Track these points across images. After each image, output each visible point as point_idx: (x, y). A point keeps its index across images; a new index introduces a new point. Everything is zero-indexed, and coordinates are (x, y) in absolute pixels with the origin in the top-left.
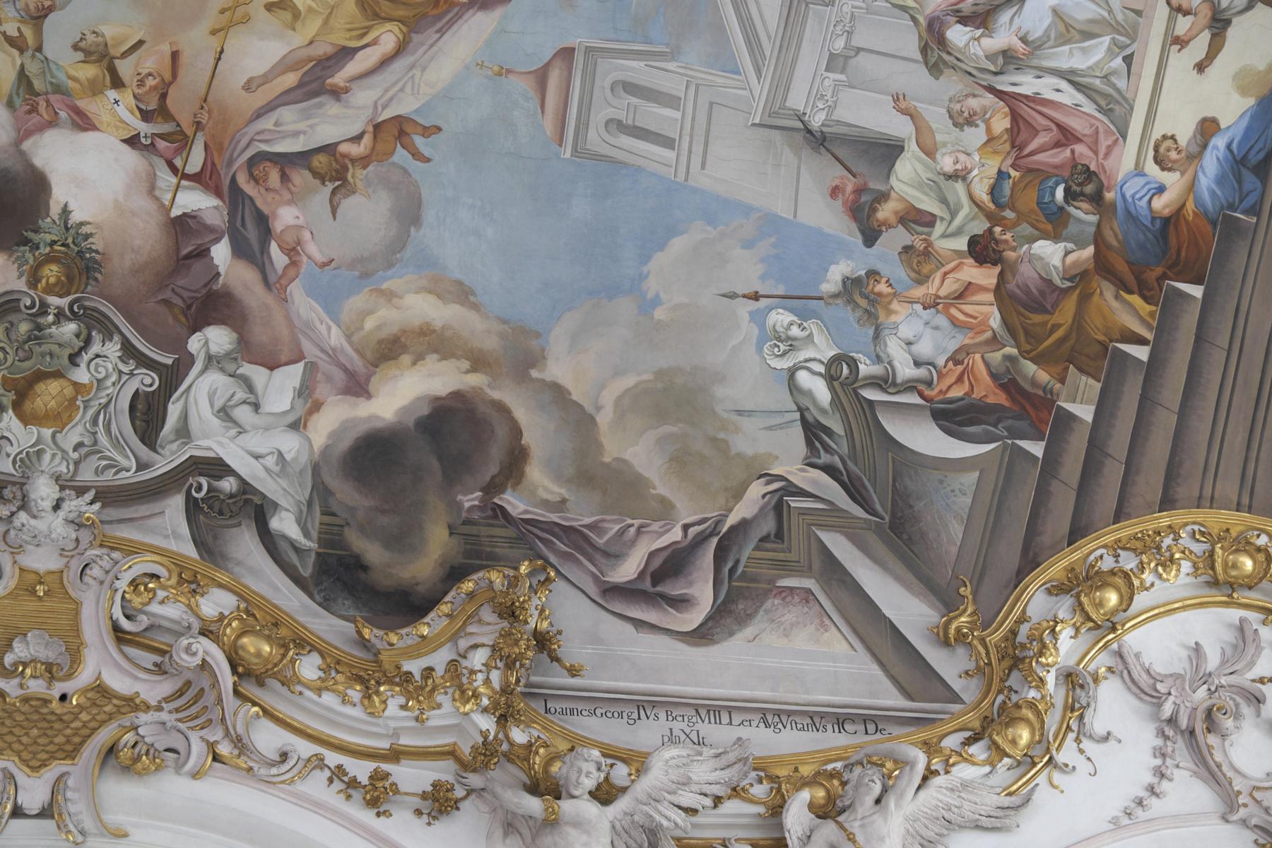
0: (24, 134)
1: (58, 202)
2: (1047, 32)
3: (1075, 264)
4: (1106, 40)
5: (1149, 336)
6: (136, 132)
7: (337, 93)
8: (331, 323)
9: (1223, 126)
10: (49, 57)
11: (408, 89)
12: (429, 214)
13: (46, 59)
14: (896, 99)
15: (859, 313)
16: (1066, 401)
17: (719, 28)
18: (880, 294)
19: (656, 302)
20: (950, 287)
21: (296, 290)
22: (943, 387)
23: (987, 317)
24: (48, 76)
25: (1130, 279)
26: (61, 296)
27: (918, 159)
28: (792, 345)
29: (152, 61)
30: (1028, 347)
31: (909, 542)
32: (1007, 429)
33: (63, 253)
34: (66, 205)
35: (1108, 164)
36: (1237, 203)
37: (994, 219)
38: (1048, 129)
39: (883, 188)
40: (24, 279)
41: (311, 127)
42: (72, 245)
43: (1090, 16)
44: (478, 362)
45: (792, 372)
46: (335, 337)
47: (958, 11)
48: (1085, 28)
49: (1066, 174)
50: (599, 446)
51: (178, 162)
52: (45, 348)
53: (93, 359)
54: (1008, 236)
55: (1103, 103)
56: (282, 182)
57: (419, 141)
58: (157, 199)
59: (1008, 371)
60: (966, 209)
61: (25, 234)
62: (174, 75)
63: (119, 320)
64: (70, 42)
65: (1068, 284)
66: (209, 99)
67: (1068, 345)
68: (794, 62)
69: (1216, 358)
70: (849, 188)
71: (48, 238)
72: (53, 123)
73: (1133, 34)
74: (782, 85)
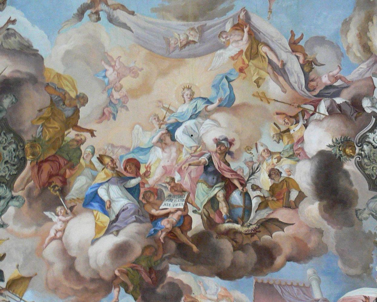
0: (306, 157)
1: (327, 148)
6: (303, 125)
7: (284, 64)
8: (359, 67)
10: (282, 150)
11: (280, 42)
12: (321, 34)
13: (283, 151)
21: (349, 78)
24: (288, 150)
26: (356, 149)
29: (280, 121)
33: (342, 147)
34: (327, 146)
40: (351, 159)
41: (296, 72)
42: (340, 145)
46: (364, 66)
51: (311, 113)
52: (372, 155)
53: (375, 141)
56: (314, 81)
57: (296, 38)
58: (323, 119)
61: (337, 158)
62: (284, 114)
63: (362, 132)
64: (277, 144)
66: (290, 103)
71: (338, 151)
72: (302, 149)
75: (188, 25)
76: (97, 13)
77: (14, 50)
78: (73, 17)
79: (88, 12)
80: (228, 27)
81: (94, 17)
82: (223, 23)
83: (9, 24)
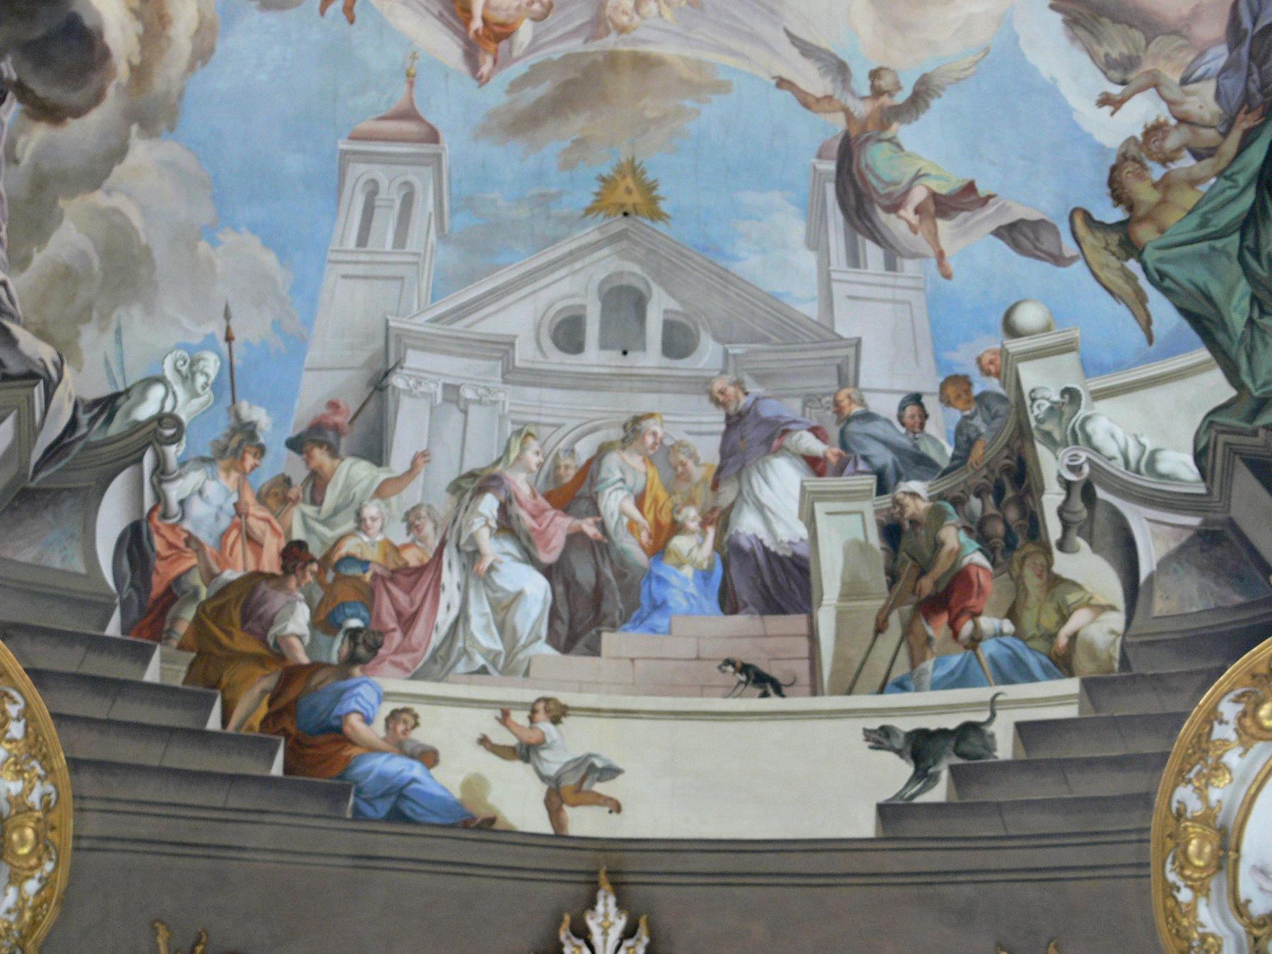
2: (503, 590)
3: (290, 647)
4: (498, 646)
5: (231, 728)
9: (433, 771)
14: (425, 454)
15: (223, 440)
16: (162, 654)
17: (471, 278)
18: (243, 459)
19: (214, 243)
20: (257, 527)
22: (164, 531)
23: (233, 567)
25: (282, 702)
27: (372, 482)
28: (187, 378)
30: (208, 609)
31: (12, 508)
32: (129, 597)
35: (386, 666)
36: (363, 796)
37: (325, 562)
38: (412, 603)
39: (342, 452)
43: (519, 627)
44: (140, 73)
45: (161, 380)
47: (510, 501)
48: (508, 626)
49: (374, 627)
50: (73, 195)
54: (310, 578)
55: (442, 653)
59: (184, 592)
60: (330, 534)
65: (271, 641)
67: (216, 651)
68: (449, 353)
69: (217, 797)
70: (338, 419)
73: (508, 671)
74: (428, 344)
75: (635, 41)
76: (877, 92)
77: (1115, 20)
78: (943, 89)
79: (901, 98)
80: (525, 32)
81: (885, 82)
82: (539, 43)
83: (1119, 98)
